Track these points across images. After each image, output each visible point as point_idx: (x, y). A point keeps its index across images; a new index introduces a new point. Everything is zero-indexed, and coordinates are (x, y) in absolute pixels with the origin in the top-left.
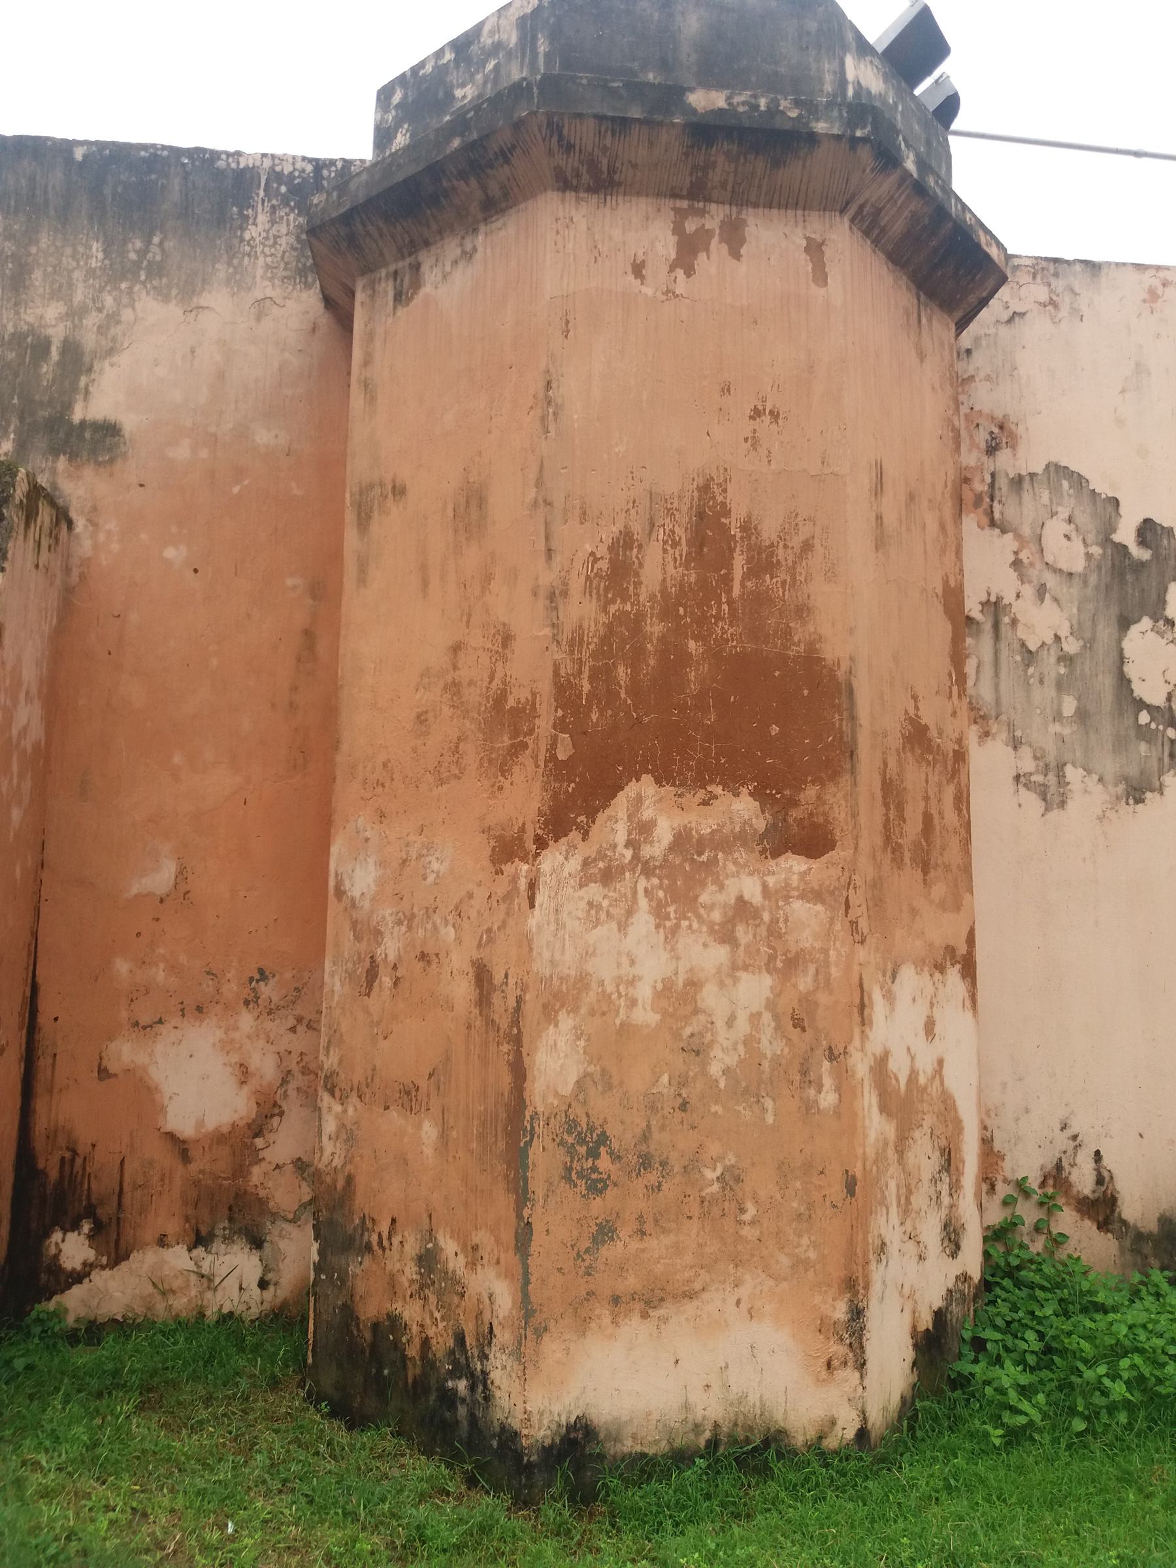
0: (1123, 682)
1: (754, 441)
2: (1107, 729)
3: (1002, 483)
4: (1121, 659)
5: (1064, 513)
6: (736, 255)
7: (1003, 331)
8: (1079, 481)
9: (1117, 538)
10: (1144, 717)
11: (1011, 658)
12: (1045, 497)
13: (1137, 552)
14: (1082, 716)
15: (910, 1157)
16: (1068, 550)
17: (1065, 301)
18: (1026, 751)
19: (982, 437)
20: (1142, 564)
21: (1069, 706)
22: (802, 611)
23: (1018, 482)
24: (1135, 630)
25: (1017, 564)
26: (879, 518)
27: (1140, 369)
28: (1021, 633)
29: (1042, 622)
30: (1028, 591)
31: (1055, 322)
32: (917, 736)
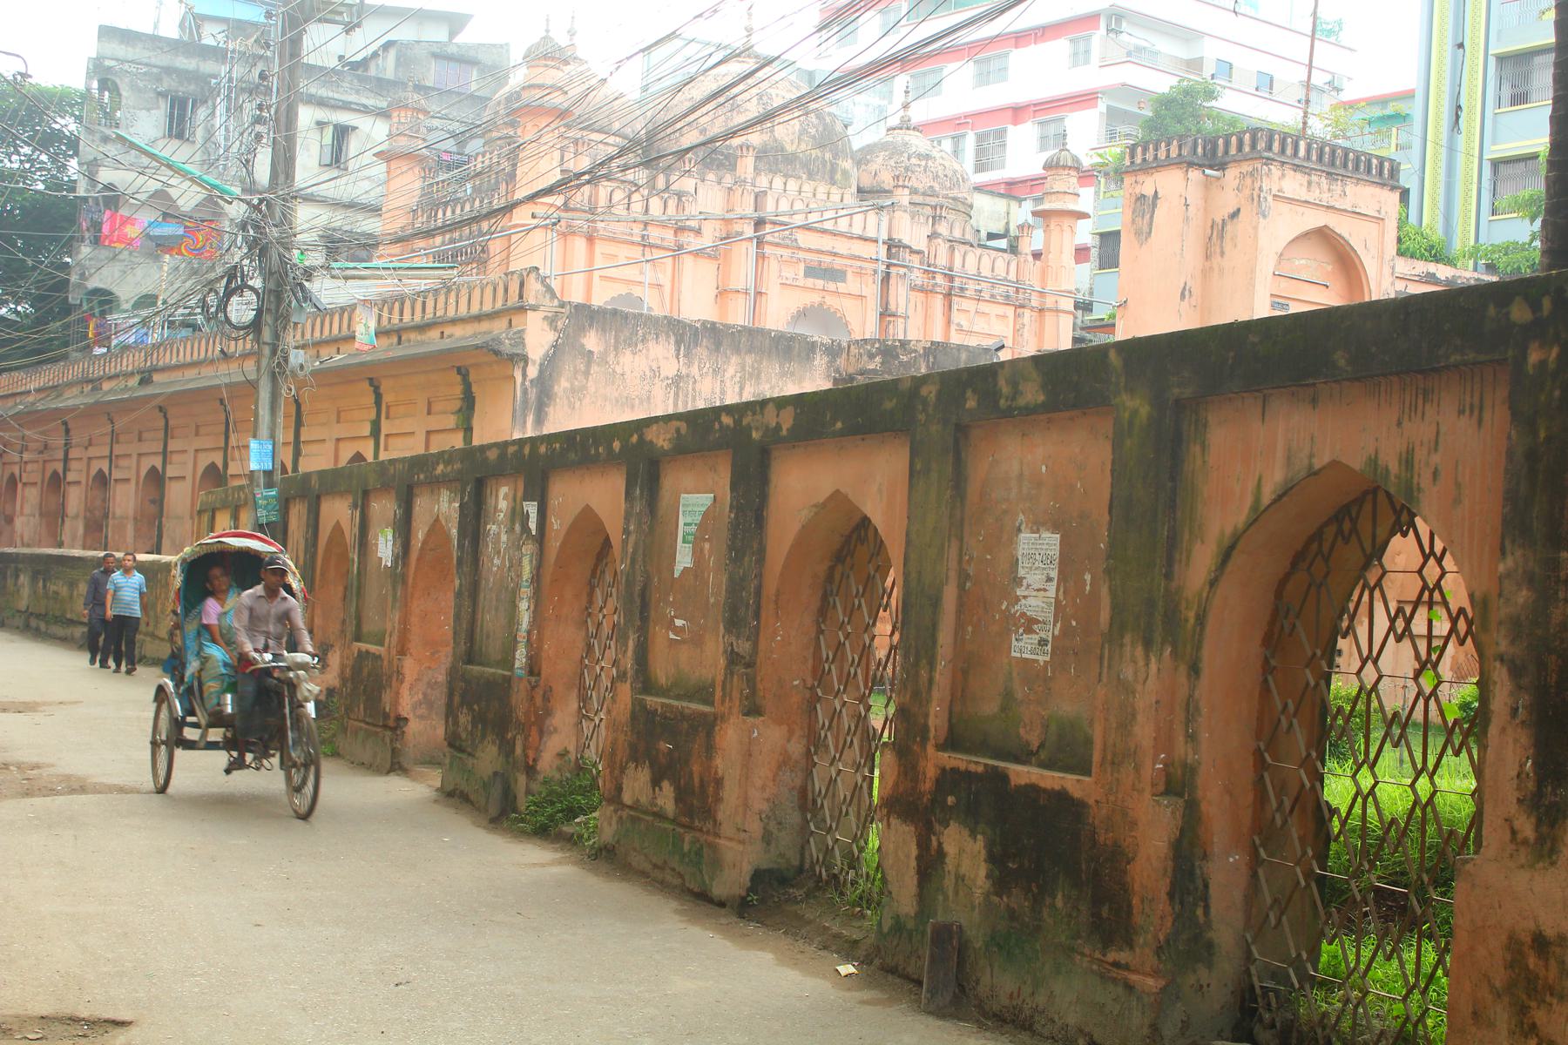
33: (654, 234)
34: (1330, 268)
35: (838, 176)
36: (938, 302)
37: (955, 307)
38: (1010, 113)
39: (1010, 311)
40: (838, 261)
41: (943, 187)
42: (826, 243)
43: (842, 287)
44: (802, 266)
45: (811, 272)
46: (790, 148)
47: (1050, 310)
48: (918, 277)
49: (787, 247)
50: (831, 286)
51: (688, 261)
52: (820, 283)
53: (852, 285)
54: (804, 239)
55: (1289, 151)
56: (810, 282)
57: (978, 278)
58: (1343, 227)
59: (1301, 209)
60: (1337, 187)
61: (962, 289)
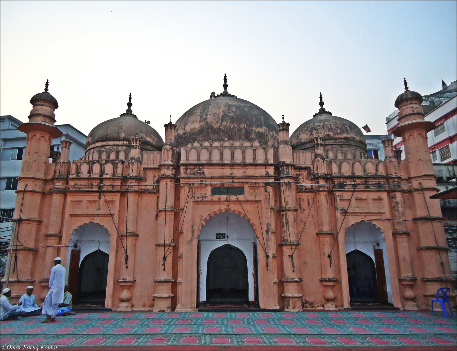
33: (107, 185)
35: (253, 136)
36: (323, 198)
37: (338, 198)
38: (449, 141)
39: (384, 196)
40: (236, 180)
42: (227, 171)
43: (241, 197)
44: (209, 188)
45: (215, 191)
46: (215, 126)
47: (417, 190)
48: (306, 183)
49: (196, 178)
50: (233, 198)
51: (132, 198)
52: (224, 197)
53: (248, 195)
54: (207, 171)
56: (216, 198)
57: (353, 177)
61: (341, 186)
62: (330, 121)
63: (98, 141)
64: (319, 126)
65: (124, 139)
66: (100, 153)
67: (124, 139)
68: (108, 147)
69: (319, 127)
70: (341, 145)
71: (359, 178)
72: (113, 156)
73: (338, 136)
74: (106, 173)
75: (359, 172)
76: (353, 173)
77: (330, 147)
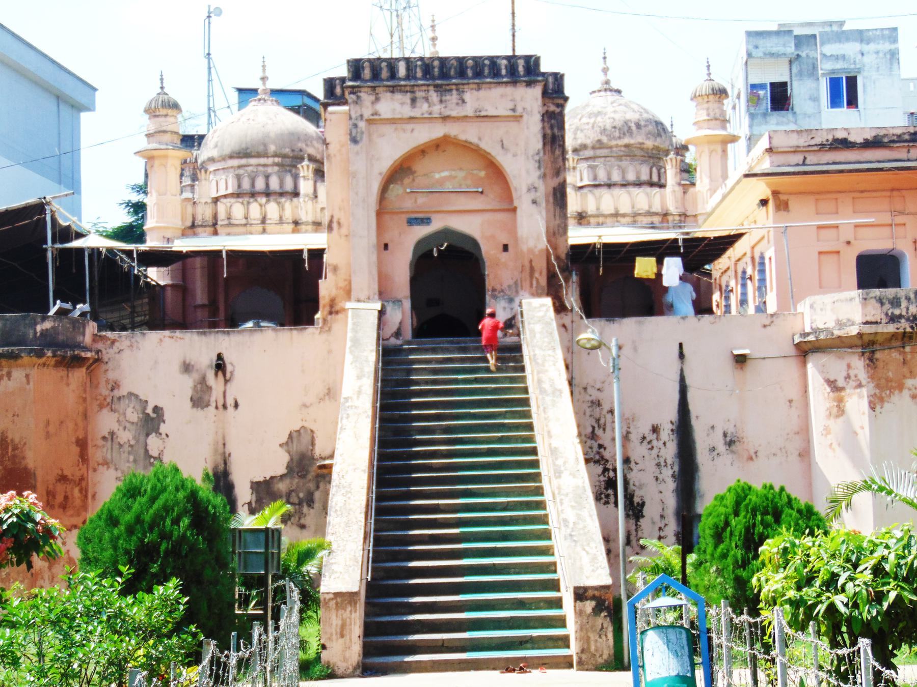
0: (147, 451)
1: (13, 422)
2: (141, 464)
3: (115, 399)
4: (146, 445)
5: (132, 406)
6: (9, 379)
7: (117, 356)
8: (137, 396)
9: (147, 411)
10: (152, 460)
11: (116, 447)
12: (127, 401)
13: (153, 415)
14: (135, 461)
15: (54, 571)
16: (133, 416)
17: (135, 344)
18: (119, 472)
19: (110, 387)
20: (153, 419)
21: (131, 458)
22: (24, 458)
23: (119, 398)
24: (150, 437)
25: (118, 421)
26: (48, 432)
27: (156, 362)
28: (119, 440)
29: (125, 436)
30: (121, 428)
31: (132, 351)
32: (63, 478)
34: (483, 174)
41: (611, 137)
55: (385, 74)
58: (469, 133)
59: (409, 127)
60: (454, 97)
62: (605, 114)
63: (231, 157)
64: (588, 123)
65: (276, 155)
66: (239, 178)
67: (276, 155)
68: (250, 169)
69: (587, 127)
70: (619, 158)
71: (624, 215)
72: (260, 185)
73: (614, 143)
74: (269, 216)
75: (625, 208)
76: (616, 209)
77: (602, 160)
